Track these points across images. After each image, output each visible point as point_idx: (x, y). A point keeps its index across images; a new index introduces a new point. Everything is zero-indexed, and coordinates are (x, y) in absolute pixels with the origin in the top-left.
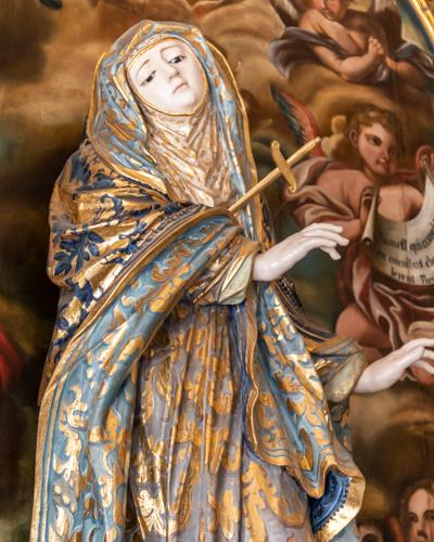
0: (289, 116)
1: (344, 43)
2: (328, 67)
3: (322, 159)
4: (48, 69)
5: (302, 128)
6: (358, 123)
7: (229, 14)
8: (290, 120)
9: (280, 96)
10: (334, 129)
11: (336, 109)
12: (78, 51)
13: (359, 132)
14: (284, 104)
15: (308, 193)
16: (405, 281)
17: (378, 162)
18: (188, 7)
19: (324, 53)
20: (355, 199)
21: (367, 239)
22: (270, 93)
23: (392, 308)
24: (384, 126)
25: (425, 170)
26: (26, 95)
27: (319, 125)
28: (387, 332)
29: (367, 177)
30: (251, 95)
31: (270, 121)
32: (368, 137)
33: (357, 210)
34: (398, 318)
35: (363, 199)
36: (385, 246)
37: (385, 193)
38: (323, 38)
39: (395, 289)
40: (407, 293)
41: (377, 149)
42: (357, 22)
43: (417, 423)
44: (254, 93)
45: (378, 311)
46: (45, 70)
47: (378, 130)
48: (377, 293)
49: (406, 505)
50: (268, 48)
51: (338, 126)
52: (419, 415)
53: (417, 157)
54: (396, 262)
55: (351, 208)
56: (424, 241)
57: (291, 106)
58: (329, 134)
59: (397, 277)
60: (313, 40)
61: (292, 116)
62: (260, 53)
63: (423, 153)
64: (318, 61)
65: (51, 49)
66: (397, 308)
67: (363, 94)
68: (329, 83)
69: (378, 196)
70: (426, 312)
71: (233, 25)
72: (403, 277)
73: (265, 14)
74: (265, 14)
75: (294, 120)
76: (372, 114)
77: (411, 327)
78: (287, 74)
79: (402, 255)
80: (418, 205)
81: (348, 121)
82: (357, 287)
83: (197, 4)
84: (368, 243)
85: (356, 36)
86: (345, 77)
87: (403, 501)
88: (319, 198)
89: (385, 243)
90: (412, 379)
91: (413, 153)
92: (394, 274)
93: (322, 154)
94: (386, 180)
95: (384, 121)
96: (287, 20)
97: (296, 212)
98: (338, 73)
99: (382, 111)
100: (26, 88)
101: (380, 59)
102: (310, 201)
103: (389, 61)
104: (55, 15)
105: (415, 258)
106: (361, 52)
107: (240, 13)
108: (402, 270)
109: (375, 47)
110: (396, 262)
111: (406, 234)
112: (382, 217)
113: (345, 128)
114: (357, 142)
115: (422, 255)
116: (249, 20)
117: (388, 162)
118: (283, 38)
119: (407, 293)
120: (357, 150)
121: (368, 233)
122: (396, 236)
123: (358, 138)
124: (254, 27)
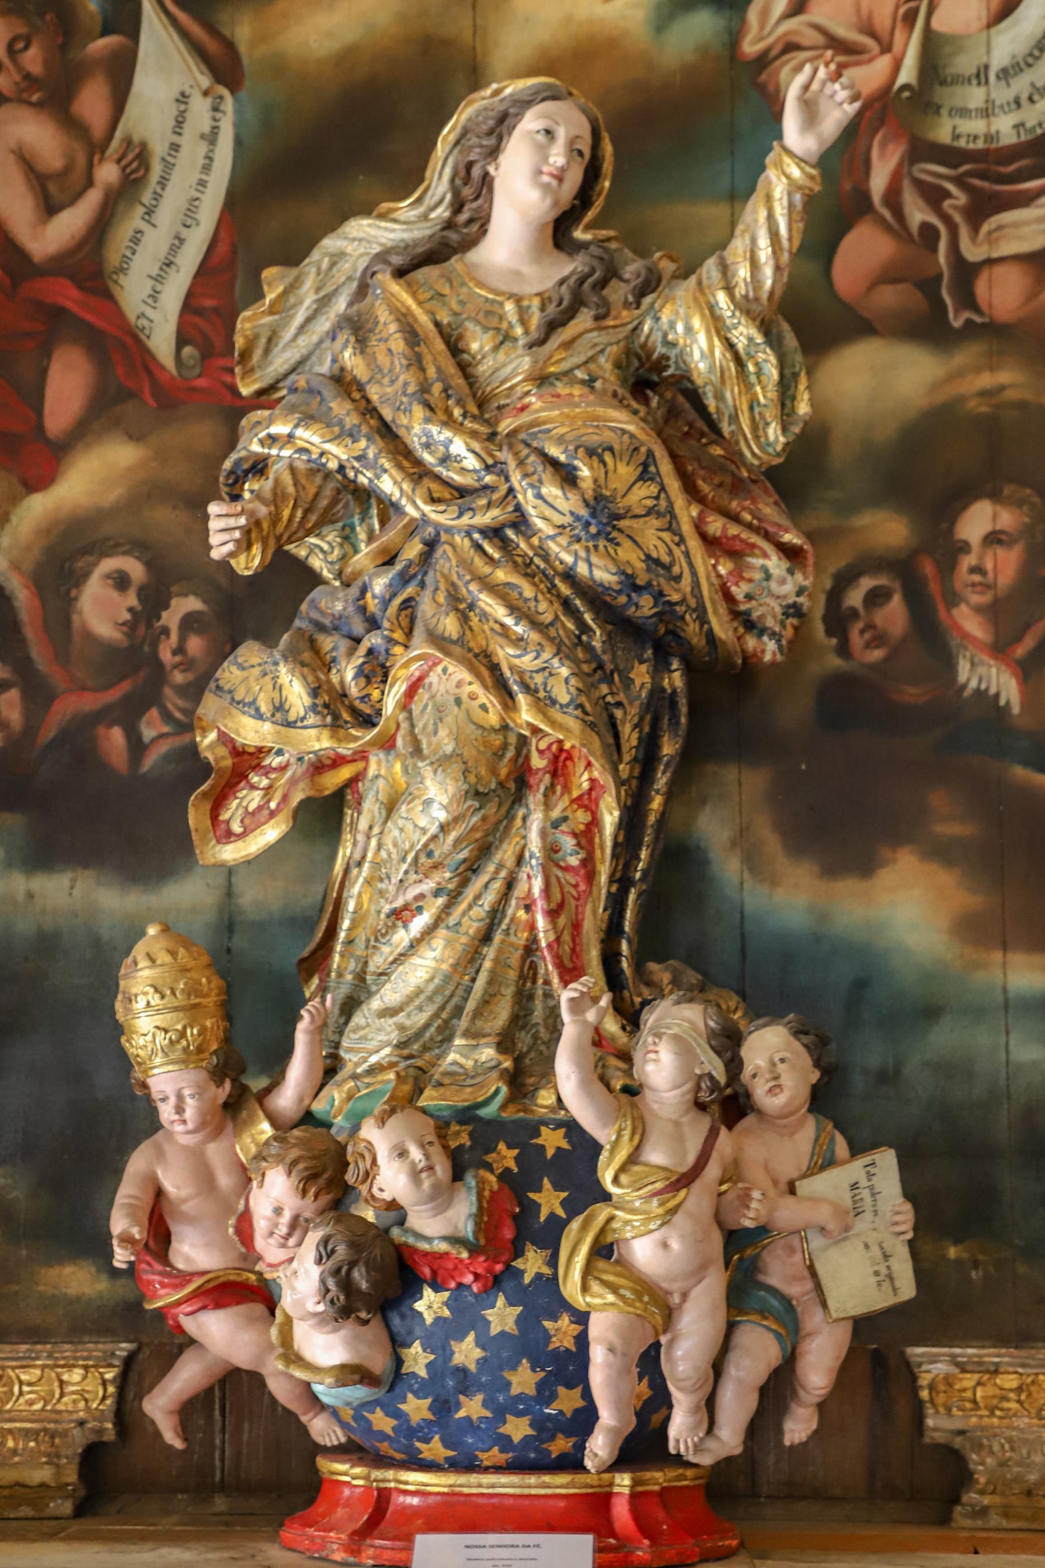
15: (787, 34)
16: (980, 145)
20: (883, 20)
21: (905, 87)
23: (947, 204)
28: (935, 249)
33: (886, 38)
34: (958, 218)
36: (947, 90)
39: (955, 166)
40: (981, 166)
43: (984, 394)
45: (918, 214)
48: (918, 183)
49: (950, 531)
52: (986, 380)
54: (964, 112)
55: (873, 34)
56: (1031, 55)
59: (962, 143)
66: (960, 198)
70: (1020, 192)
72: (976, 138)
77: (985, 228)
79: (975, 96)
82: (878, 182)
84: (906, 94)
87: (944, 526)
88: (812, 37)
89: (943, 83)
90: (978, 320)
92: (956, 137)
97: (763, 77)
102: (791, 47)
105: (1002, 94)
108: (976, 126)
110: (964, 112)
111: (988, 52)
112: (936, 33)
115: (1021, 85)
119: (981, 166)
121: (907, 74)
122: (965, 63)
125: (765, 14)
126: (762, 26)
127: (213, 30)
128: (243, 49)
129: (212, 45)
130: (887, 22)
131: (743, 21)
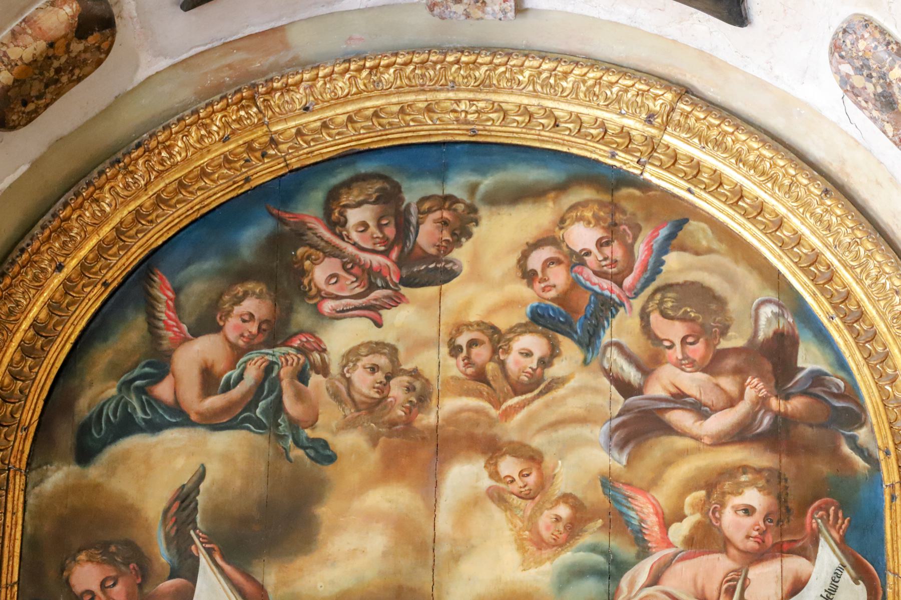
0: (625, 510)
1: (709, 398)
2: (682, 434)
3: (670, 551)
4: (323, 534)
5: (642, 520)
6: (724, 494)
7: (547, 406)
8: (628, 516)
9: (613, 488)
10: (687, 511)
11: (690, 486)
12: (357, 504)
13: (723, 505)
14: (619, 497)
17: (748, 537)
18: (494, 413)
19: (680, 418)
22: (600, 489)
24: (760, 489)
25: (819, 531)
26: (301, 570)
27: (666, 511)
29: (734, 560)
30: (575, 498)
31: (600, 521)
32: (736, 510)
35: (724, 587)
37: (755, 573)
38: (679, 398)
41: (748, 521)
42: (730, 362)
44: (579, 495)
46: (320, 537)
47: (753, 497)
50: (599, 433)
51: (693, 506)
53: (809, 514)
57: (627, 497)
58: (681, 517)
60: (663, 405)
61: (629, 508)
62: (588, 442)
63: (820, 508)
64: (670, 430)
65: (324, 512)
67: (733, 455)
68: (684, 453)
69: (745, 578)
71: (552, 417)
73: (596, 391)
74: (596, 391)
75: (632, 514)
76: (743, 478)
78: (624, 460)
80: (803, 579)
81: (709, 495)
83: (504, 407)
85: (728, 384)
86: (707, 441)
91: (802, 513)
93: (670, 545)
94: (758, 557)
95: (761, 483)
96: (625, 388)
98: (697, 438)
99: (759, 471)
100: (301, 561)
101: (762, 403)
103: (774, 403)
104: (329, 470)
106: (731, 403)
107: (564, 398)
109: (755, 388)
113: (702, 507)
114: (719, 520)
116: (574, 405)
117: (763, 533)
118: (619, 415)
120: (720, 529)
123: (721, 513)
124: (581, 412)
125: (632, 584)
126: (630, 592)
127: (249, 577)
128: (270, 590)
129: (248, 587)
130: (715, 594)
131: (618, 587)
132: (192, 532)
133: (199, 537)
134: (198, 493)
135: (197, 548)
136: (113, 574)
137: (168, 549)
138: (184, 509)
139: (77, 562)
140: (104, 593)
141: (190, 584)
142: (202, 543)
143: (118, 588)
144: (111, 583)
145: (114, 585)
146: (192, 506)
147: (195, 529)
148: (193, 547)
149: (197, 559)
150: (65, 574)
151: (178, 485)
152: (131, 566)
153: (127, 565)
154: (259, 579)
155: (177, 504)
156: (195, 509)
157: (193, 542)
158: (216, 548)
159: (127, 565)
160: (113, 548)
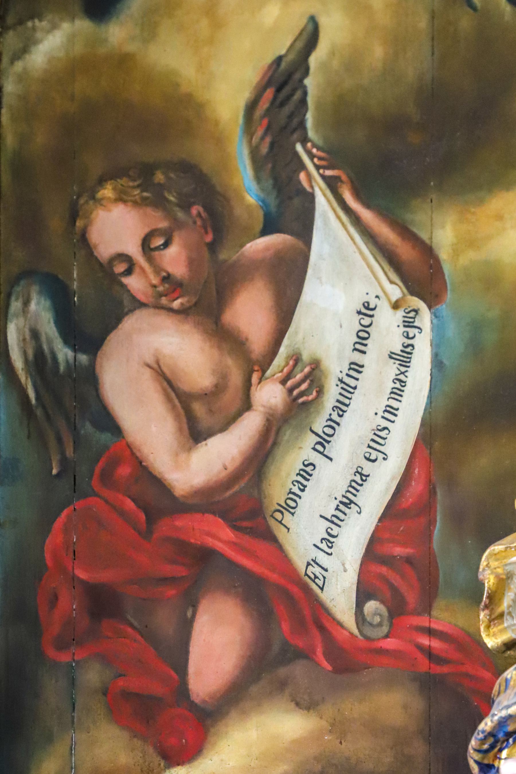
26: (500, 217)
132: (299, 148)
133: (311, 156)
134: (306, 72)
135: (309, 176)
136: (163, 224)
137: (258, 178)
138: (282, 104)
139: (99, 202)
140: (150, 259)
141: (300, 244)
142: (318, 168)
143: (173, 250)
144: (159, 241)
145: (166, 245)
146: (298, 95)
147: (304, 140)
148: (302, 176)
149: (311, 198)
150: (79, 223)
151: (270, 58)
152: (195, 210)
153: (186, 207)
154: (424, 236)
155: (269, 93)
156: (303, 102)
157: (303, 167)
158: (344, 178)
159: (186, 207)
160: (159, 177)
